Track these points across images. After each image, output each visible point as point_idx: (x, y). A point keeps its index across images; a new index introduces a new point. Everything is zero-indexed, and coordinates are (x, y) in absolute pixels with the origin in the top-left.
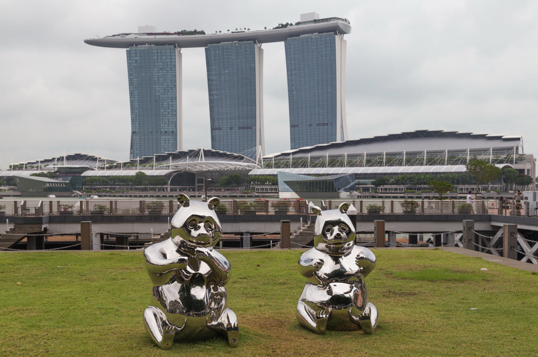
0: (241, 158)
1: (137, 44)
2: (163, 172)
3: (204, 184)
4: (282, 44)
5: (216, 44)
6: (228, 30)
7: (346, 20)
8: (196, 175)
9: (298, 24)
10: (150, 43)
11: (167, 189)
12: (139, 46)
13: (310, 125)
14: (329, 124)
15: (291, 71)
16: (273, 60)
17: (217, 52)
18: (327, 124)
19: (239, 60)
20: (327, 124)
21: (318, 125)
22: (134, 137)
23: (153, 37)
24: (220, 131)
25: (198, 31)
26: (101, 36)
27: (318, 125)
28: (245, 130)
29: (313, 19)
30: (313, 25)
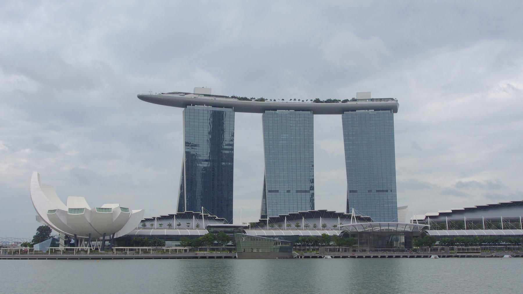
0: (369, 220)
1: (194, 103)
2: (338, 233)
4: (338, 118)
6: (283, 100)
9: (354, 100)
11: (339, 250)
13: (370, 191)
14: (389, 191)
18: (387, 191)
19: (297, 128)
20: (387, 191)
23: (213, 98)
26: (155, 92)
27: (378, 191)
28: (303, 193)
30: (372, 102)
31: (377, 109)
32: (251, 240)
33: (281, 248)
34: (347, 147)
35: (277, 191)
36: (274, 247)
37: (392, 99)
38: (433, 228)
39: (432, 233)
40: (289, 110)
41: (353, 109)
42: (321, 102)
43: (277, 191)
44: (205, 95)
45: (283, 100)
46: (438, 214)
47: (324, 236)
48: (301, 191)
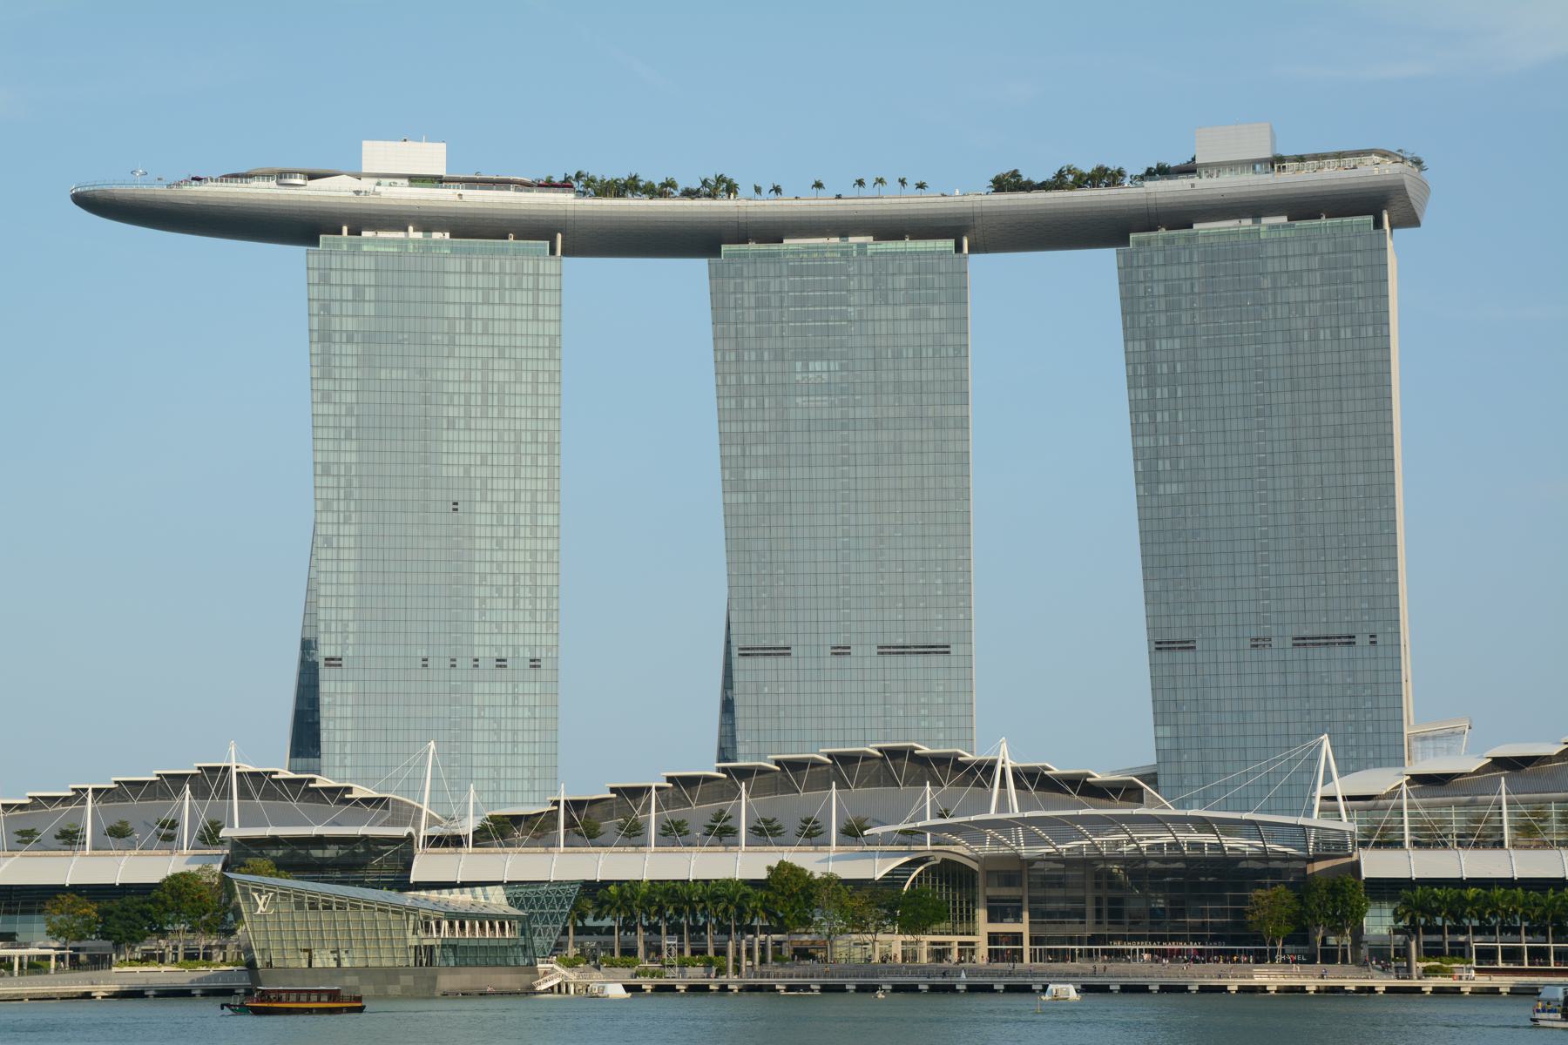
3: (1023, 927)
5: (763, 247)
7: (1418, 162)
8: (981, 882)
10: (428, 222)
12: (365, 234)
15: (1152, 385)
16: (1049, 332)
17: (774, 285)
18: (1350, 640)
20: (1350, 640)
21: (1301, 642)
22: (325, 687)
24: (781, 659)
25: (645, 178)
27: (1301, 642)
29: (1267, 154)
31: (1303, 207)
32: (299, 905)
33: (451, 947)
34: (1145, 418)
35: (784, 651)
36: (413, 941)
37: (1385, 154)
38: (1428, 840)
39: (1376, 864)
40: (844, 234)
41: (1180, 217)
42: (1029, 187)
43: (784, 651)
44: (414, 180)
45: (818, 185)
46: (1468, 763)
47: (784, 876)
48: (903, 650)
